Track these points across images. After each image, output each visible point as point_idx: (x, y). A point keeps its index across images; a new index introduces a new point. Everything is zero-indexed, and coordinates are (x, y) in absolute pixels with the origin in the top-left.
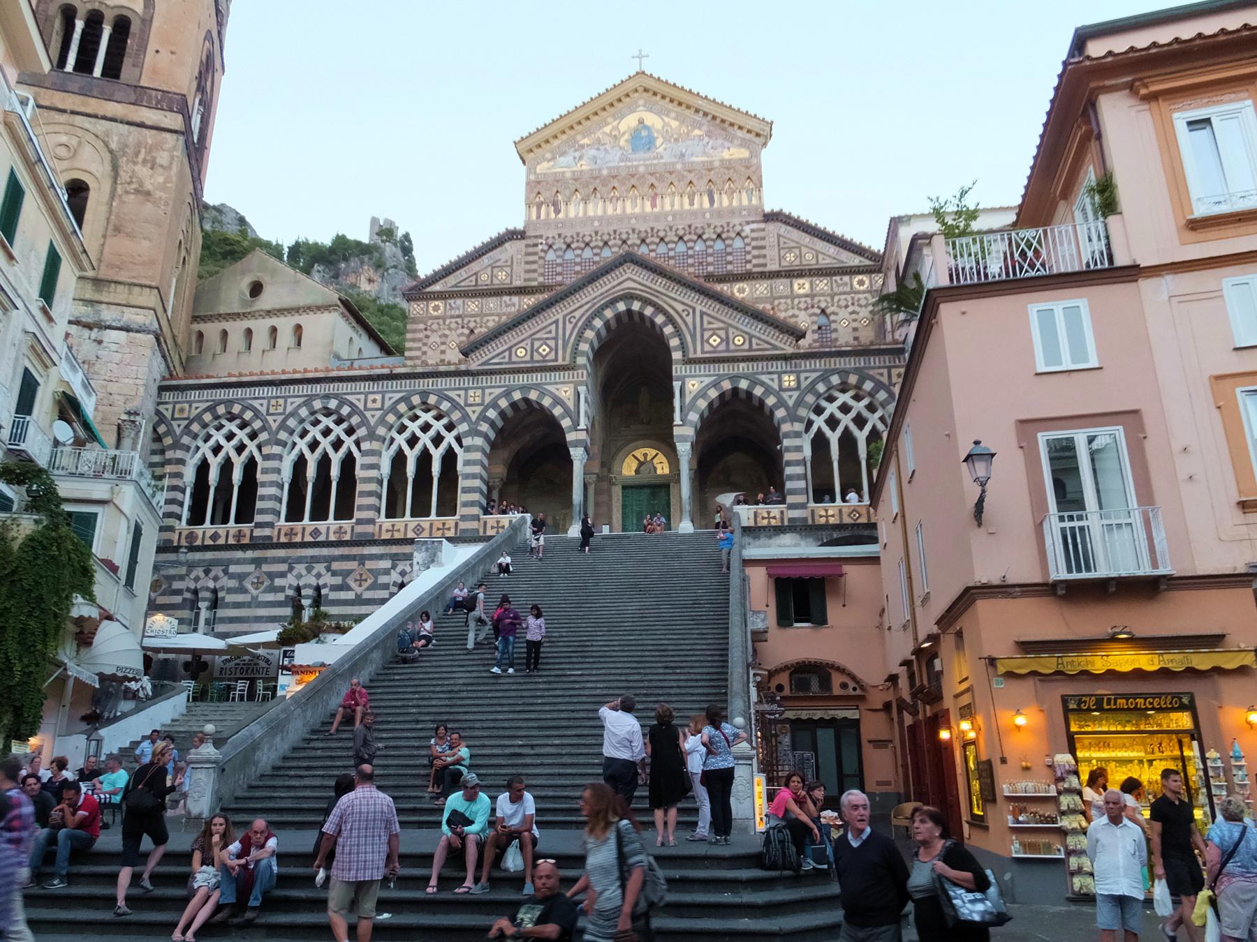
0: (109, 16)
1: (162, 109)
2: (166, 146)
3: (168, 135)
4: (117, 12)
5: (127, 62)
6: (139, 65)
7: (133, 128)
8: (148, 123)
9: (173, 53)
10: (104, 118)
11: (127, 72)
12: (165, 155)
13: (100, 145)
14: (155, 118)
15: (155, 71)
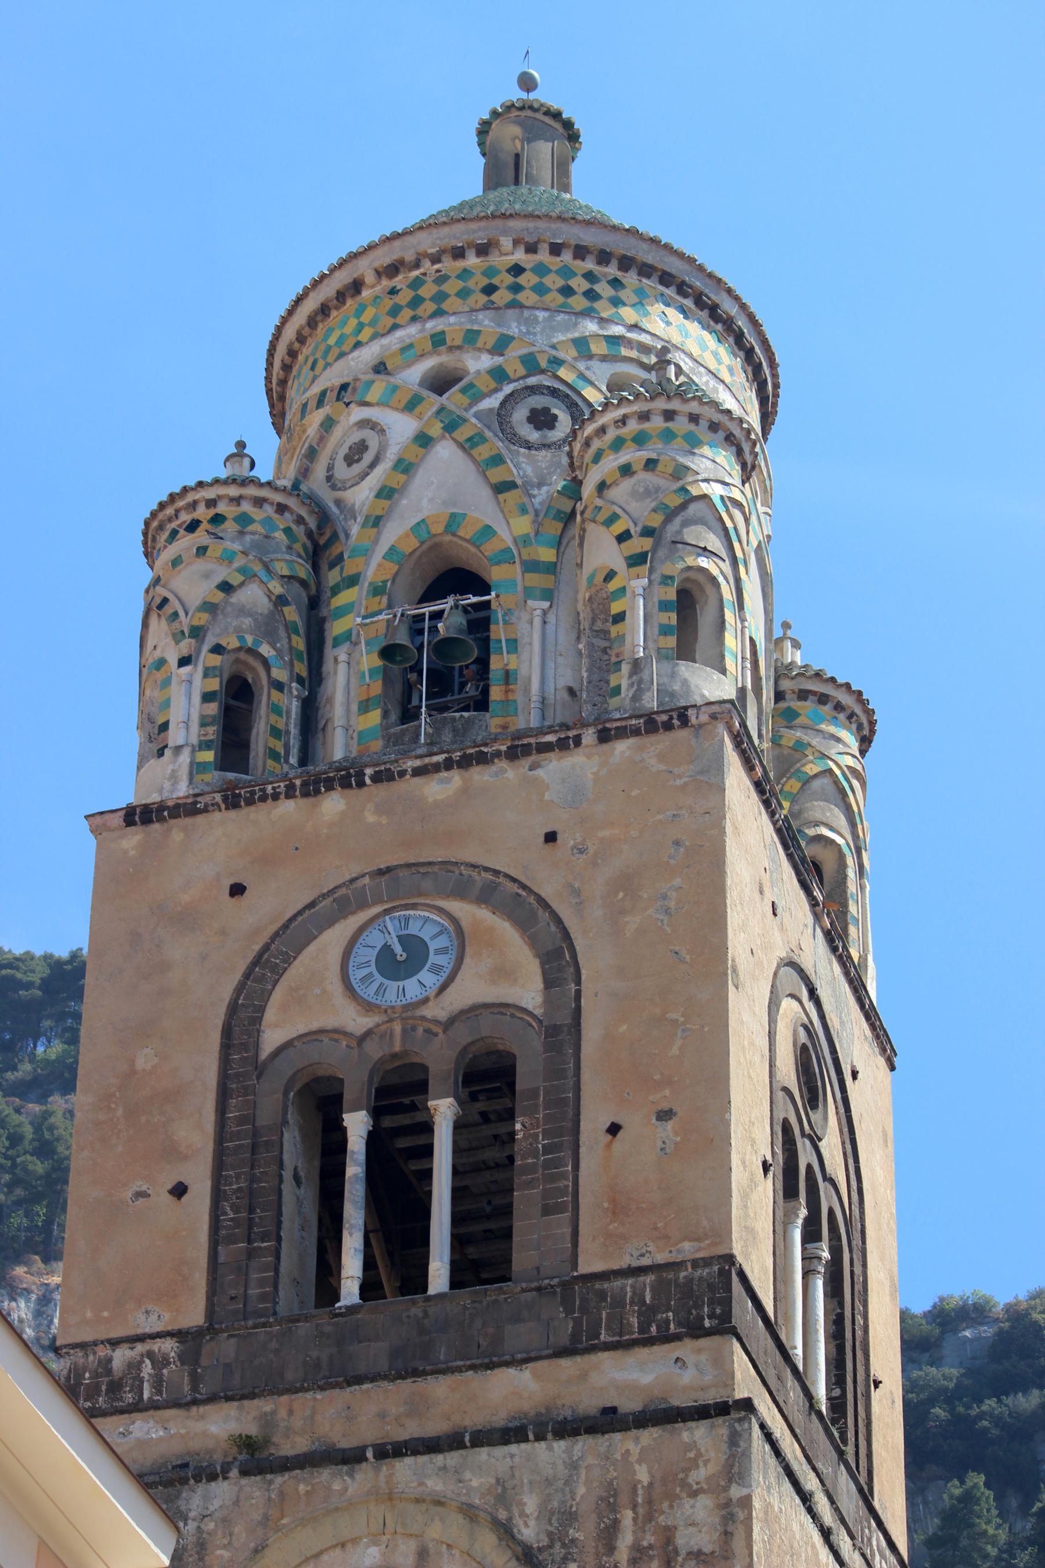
0: (440, 1058)
1: (666, 1338)
2: (700, 1475)
3: (700, 1434)
4: (463, 1035)
5: (526, 1200)
6: (564, 1203)
7: (582, 1445)
8: (629, 1405)
9: (665, 1115)
10: (483, 1438)
11: (532, 1242)
12: (702, 1509)
13: (487, 1541)
14: (646, 1379)
15: (618, 1207)
